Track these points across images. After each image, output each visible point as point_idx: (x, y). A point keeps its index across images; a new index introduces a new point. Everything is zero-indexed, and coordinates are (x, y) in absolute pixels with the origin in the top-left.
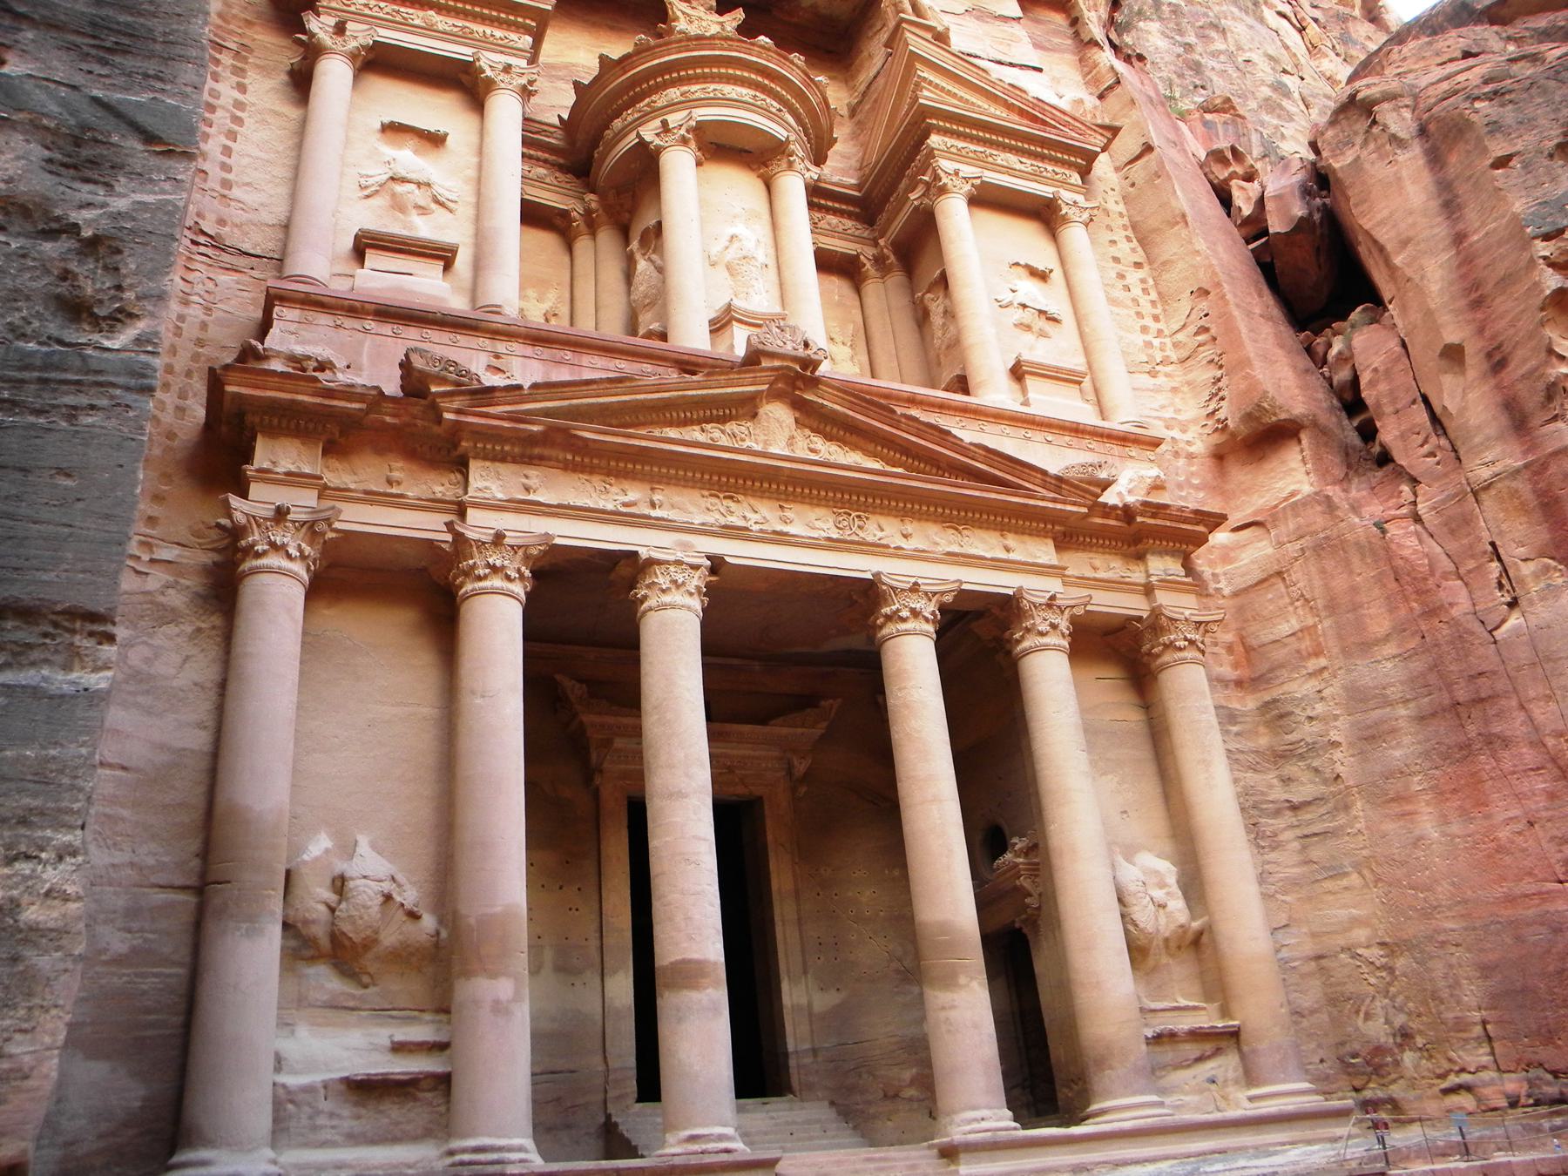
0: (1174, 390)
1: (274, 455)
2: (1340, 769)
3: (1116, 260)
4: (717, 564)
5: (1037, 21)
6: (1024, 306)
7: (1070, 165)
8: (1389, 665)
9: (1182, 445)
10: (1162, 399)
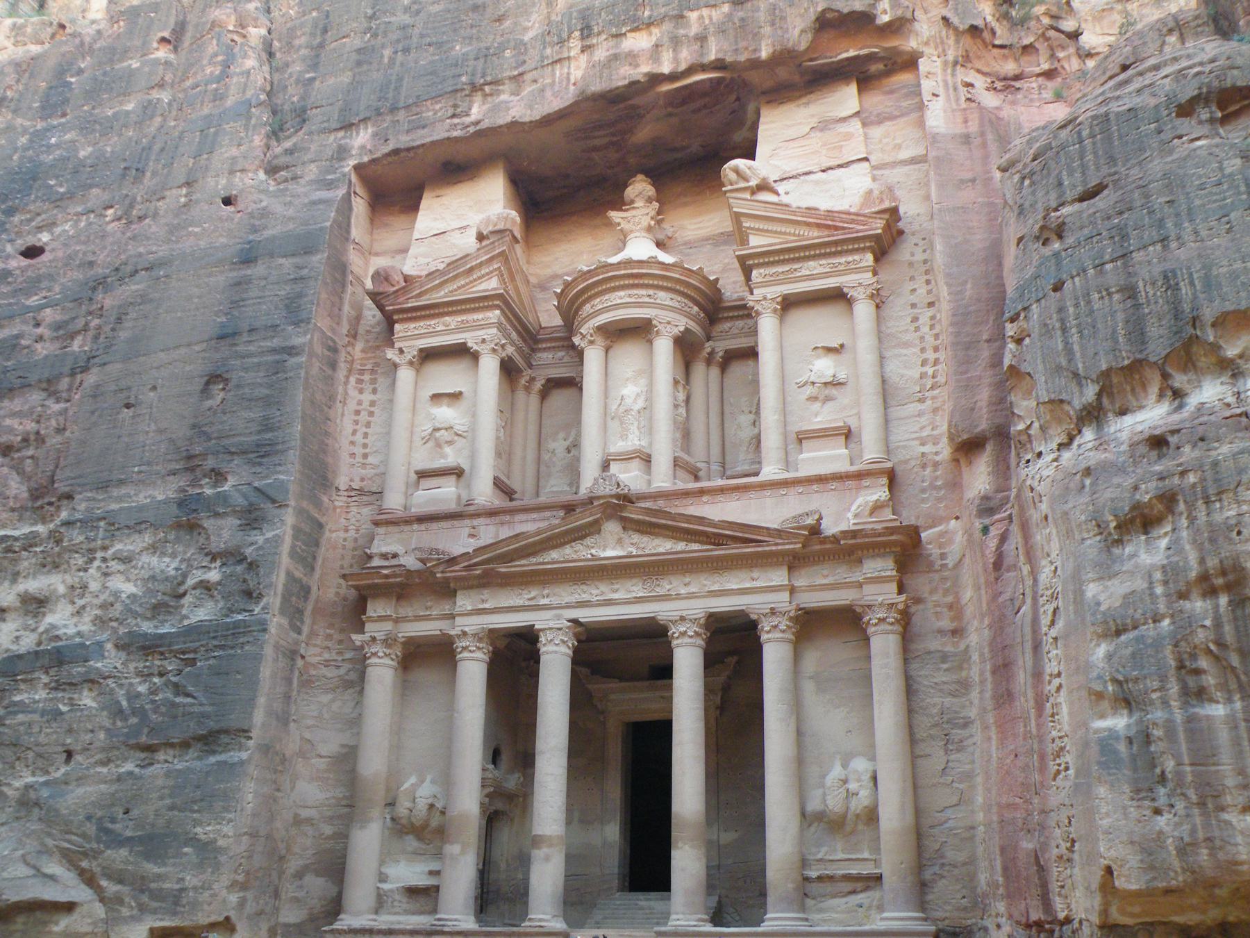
0: (935, 410)
1: (376, 608)
3: (913, 306)
4: (575, 621)
5: (891, 92)
6: (813, 383)
7: (863, 250)
10: (924, 420)
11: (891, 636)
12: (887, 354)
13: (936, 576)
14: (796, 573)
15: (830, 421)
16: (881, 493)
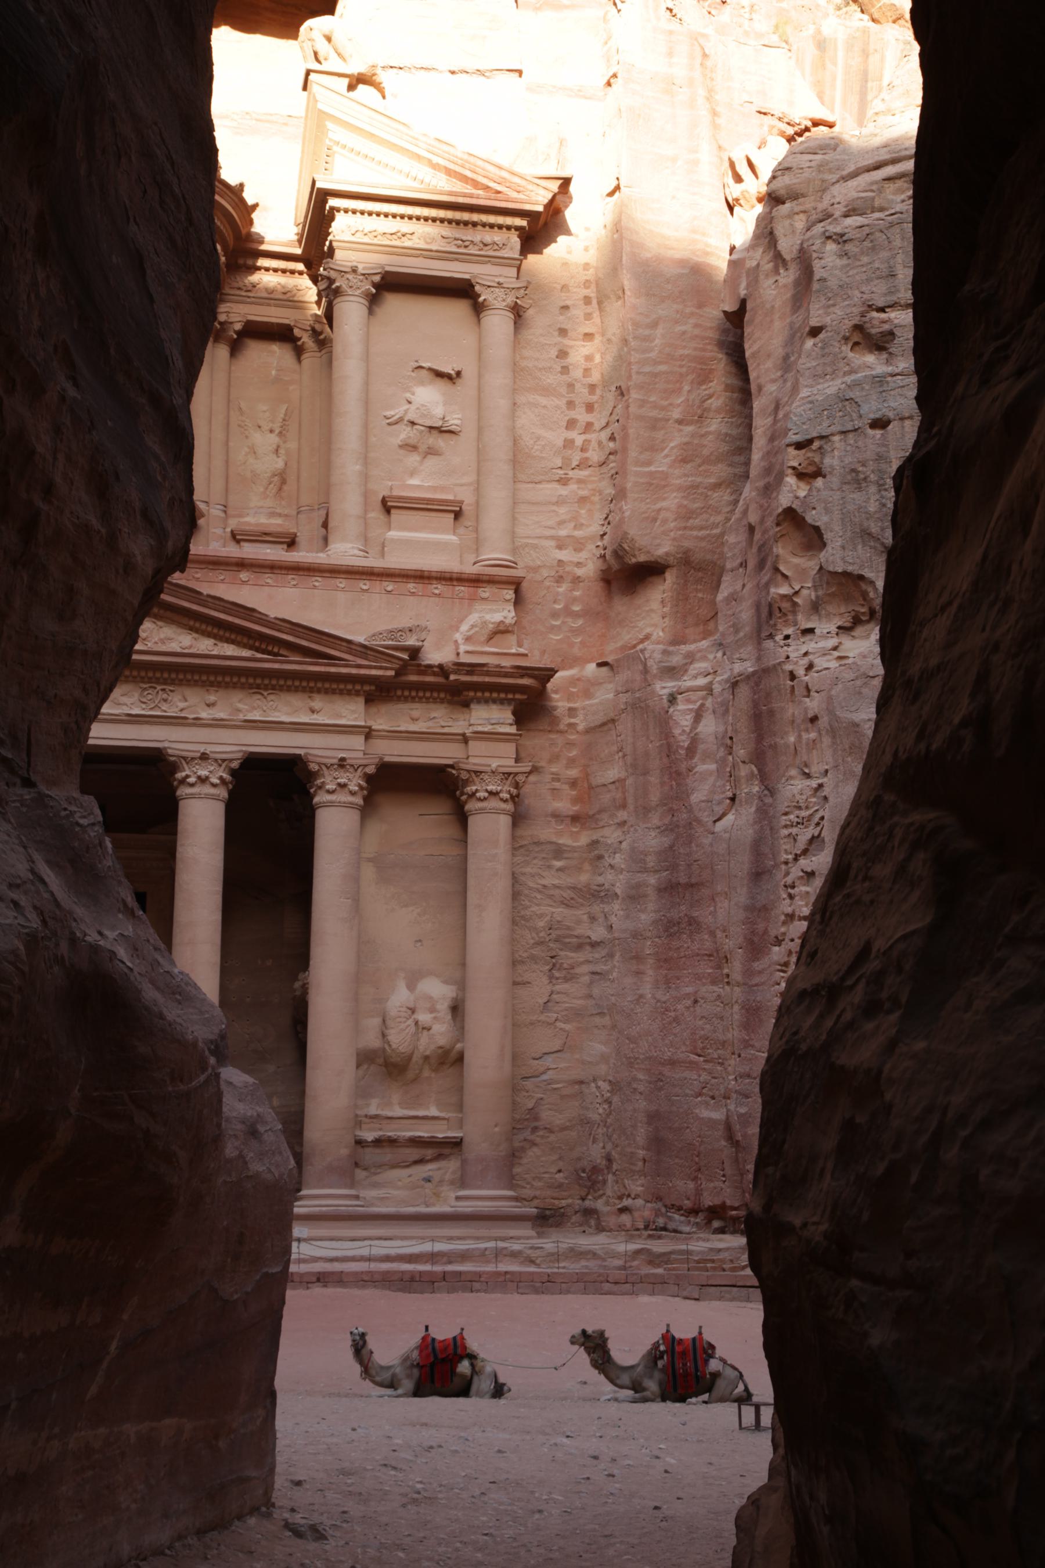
0: (583, 500)
2: (613, 919)
3: (563, 332)
6: (413, 423)
8: (653, 834)
9: (568, 569)
10: (562, 510)
11: (502, 816)
12: (521, 399)
13: (560, 740)
14: (373, 710)
15: (434, 489)
16: (505, 614)
